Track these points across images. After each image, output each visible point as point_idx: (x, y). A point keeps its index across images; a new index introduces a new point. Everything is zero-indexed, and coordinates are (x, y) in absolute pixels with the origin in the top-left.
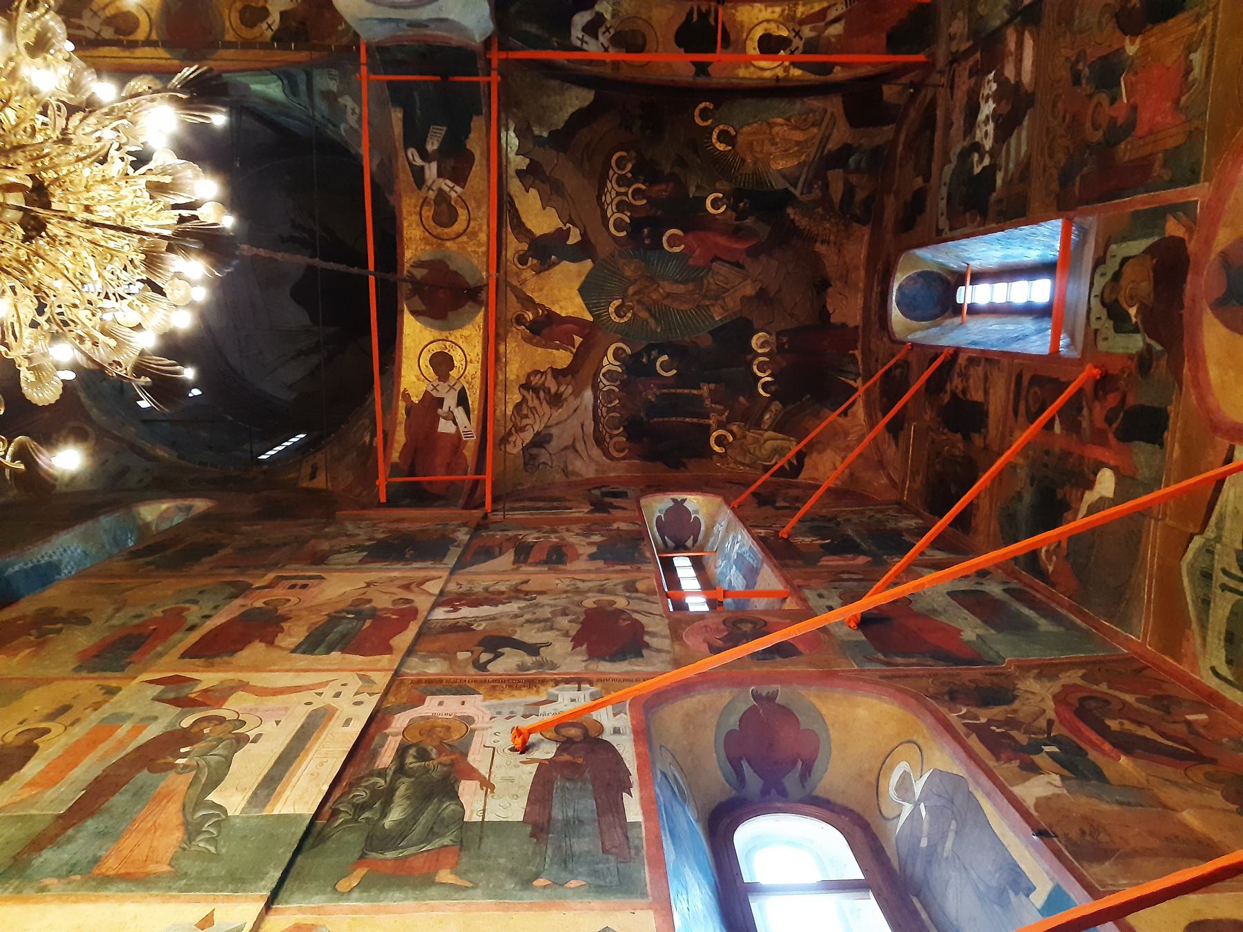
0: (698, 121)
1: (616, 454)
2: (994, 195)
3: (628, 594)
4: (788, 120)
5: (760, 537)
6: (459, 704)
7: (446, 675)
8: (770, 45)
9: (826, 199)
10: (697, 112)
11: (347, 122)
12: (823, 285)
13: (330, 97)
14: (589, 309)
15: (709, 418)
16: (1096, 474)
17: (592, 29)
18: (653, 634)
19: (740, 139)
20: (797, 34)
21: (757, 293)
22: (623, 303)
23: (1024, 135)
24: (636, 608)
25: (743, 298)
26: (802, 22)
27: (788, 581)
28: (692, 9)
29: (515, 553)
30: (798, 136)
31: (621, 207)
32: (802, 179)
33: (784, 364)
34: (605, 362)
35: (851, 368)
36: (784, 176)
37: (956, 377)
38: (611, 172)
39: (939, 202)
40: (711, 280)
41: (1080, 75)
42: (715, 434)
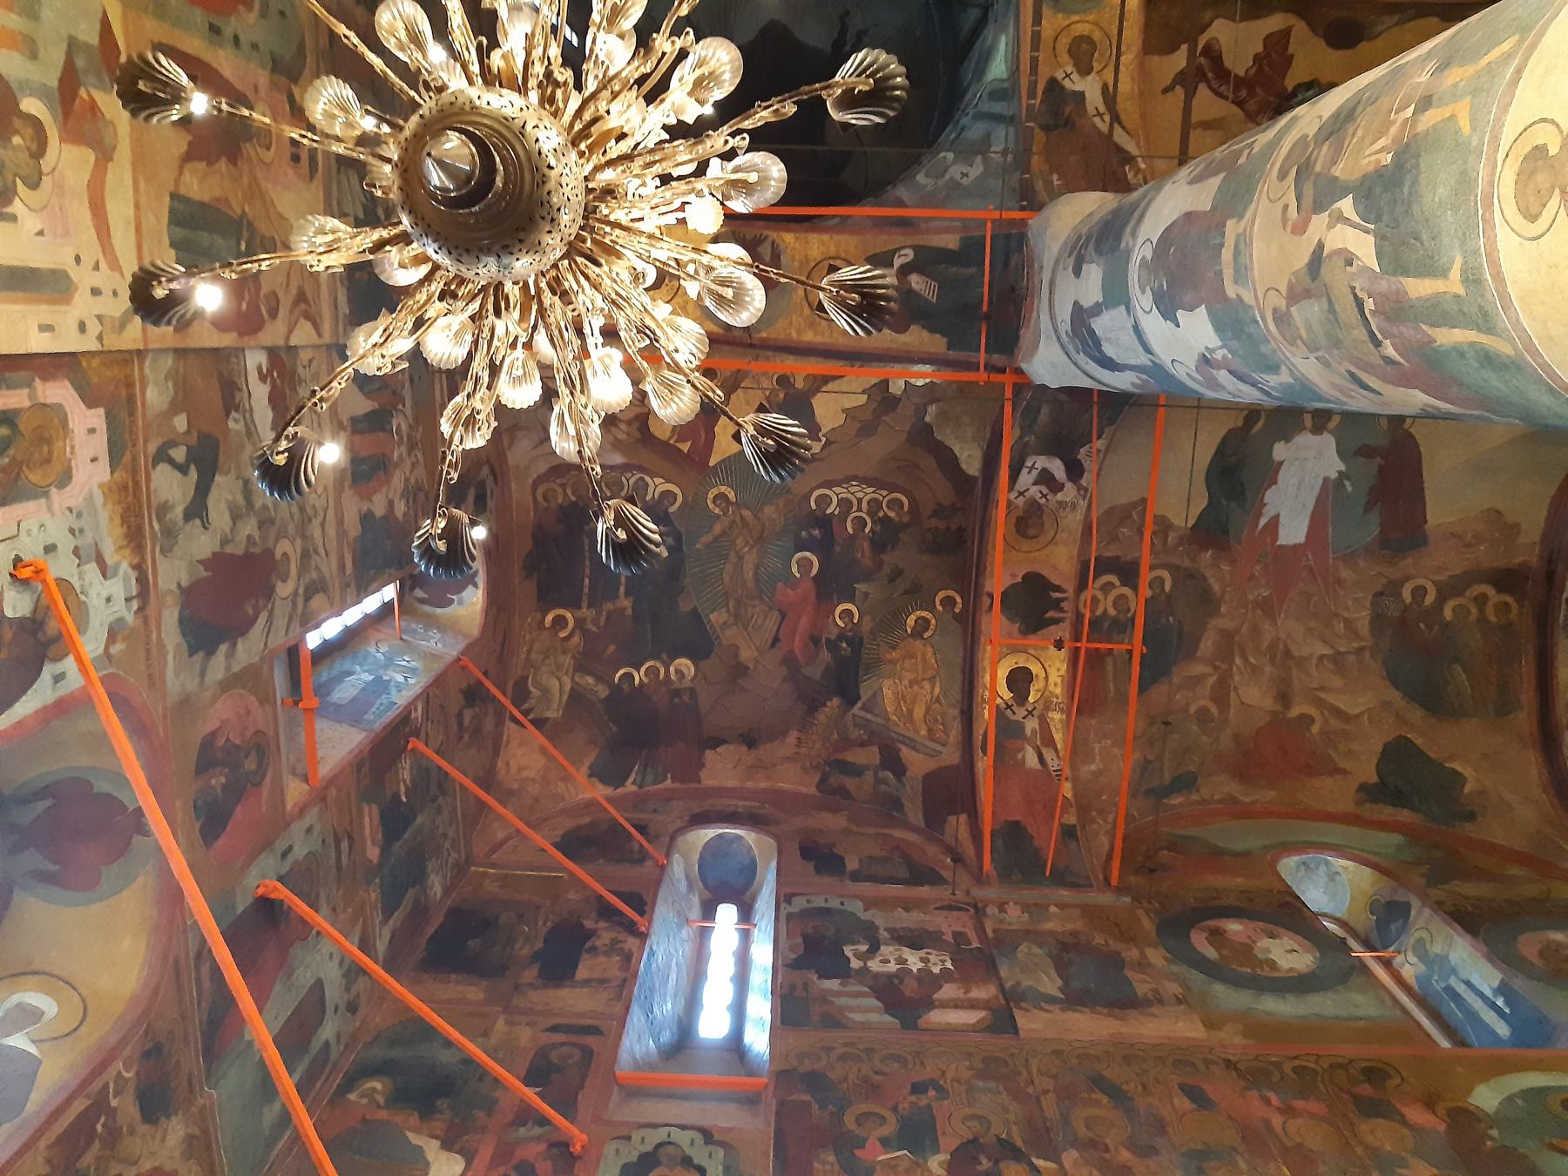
0: (942, 594)
1: (540, 490)
2: (815, 977)
3: (301, 591)
4: (938, 700)
5: (410, 713)
6: (91, 456)
7: (144, 415)
8: (1020, 680)
9: (847, 743)
10: (951, 593)
11: (954, 162)
12: (750, 740)
13: (983, 147)
14: (724, 461)
15: (589, 607)
16: (459, 1152)
17: (1046, 478)
18: (231, 654)
19: (918, 644)
20: (1030, 713)
21: (739, 664)
22: (732, 503)
23: (873, 1017)
24: (277, 612)
25: (737, 648)
26: (1043, 721)
27: (332, 781)
28: (1065, 592)
29: (373, 412)
30: (919, 713)
31: (845, 504)
32: (869, 716)
33: (655, 699)
34: (658, 480)
35: (649, 778)
36: (874, 695)
37: (613, 935)
38: (884, 493)
39: (827, 894)
40: (757, 609)
41: (921, 1093)
42: (569, 615)
